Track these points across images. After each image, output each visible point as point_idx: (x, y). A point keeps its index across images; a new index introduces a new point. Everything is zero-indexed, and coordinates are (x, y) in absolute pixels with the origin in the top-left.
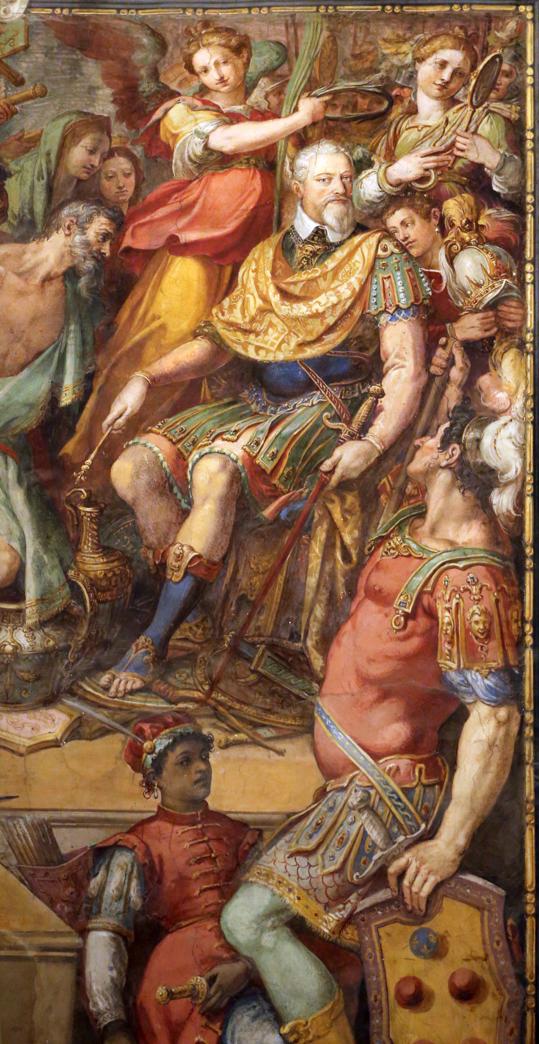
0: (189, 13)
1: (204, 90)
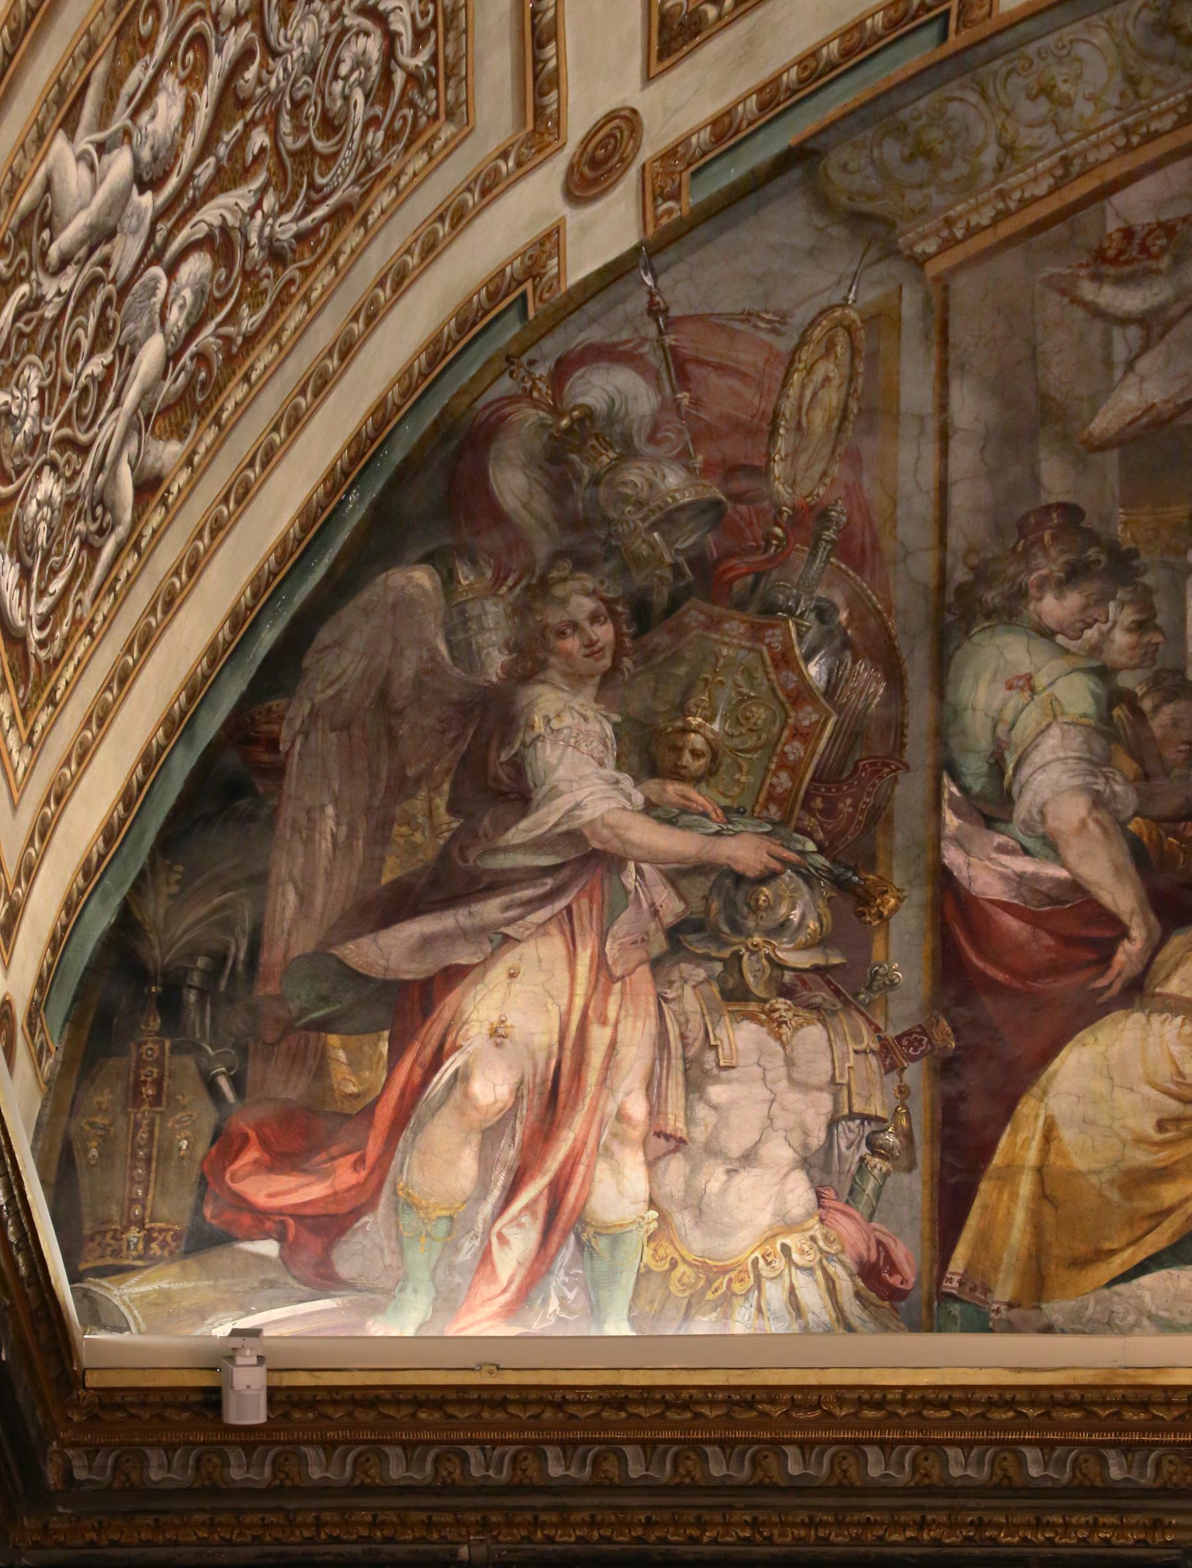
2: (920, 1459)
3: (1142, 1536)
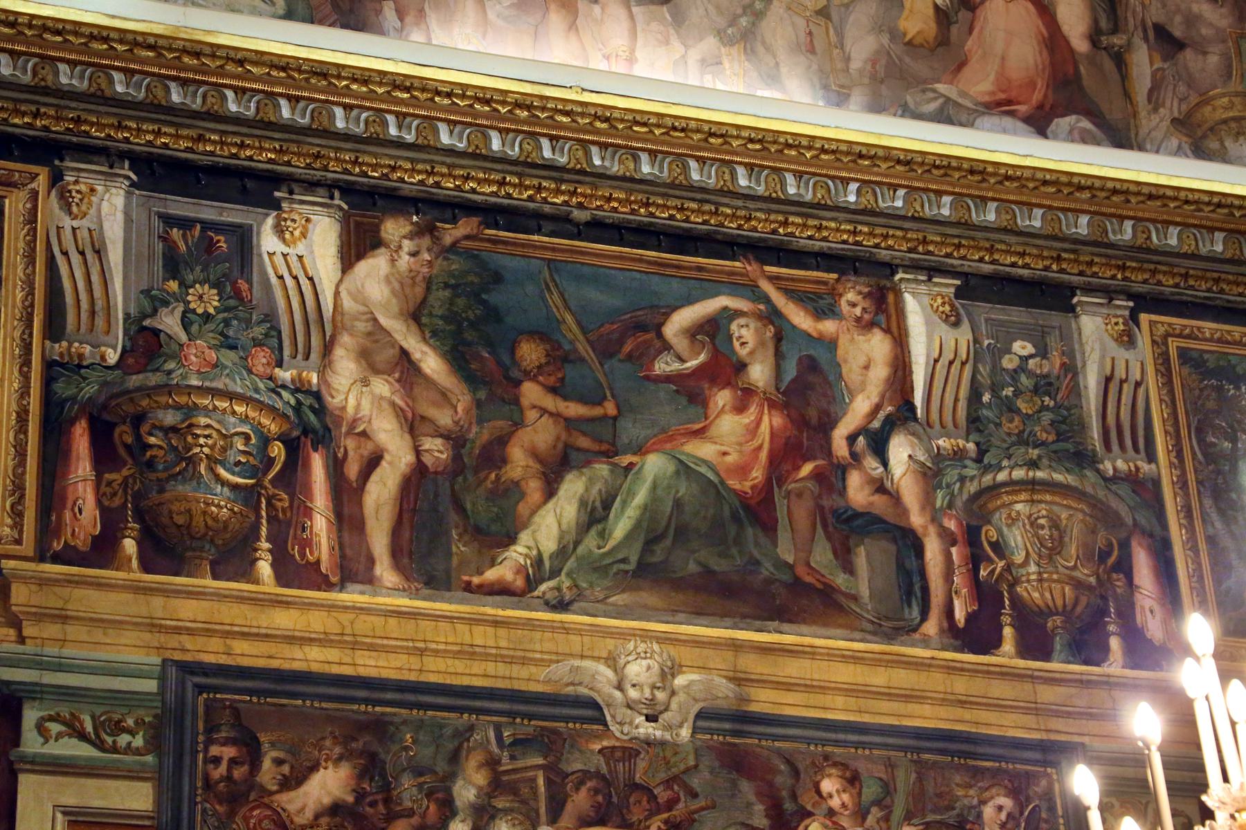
0: (812, 748)
1: (831, 813)
2: (39, 68)
3: (190, 145)
